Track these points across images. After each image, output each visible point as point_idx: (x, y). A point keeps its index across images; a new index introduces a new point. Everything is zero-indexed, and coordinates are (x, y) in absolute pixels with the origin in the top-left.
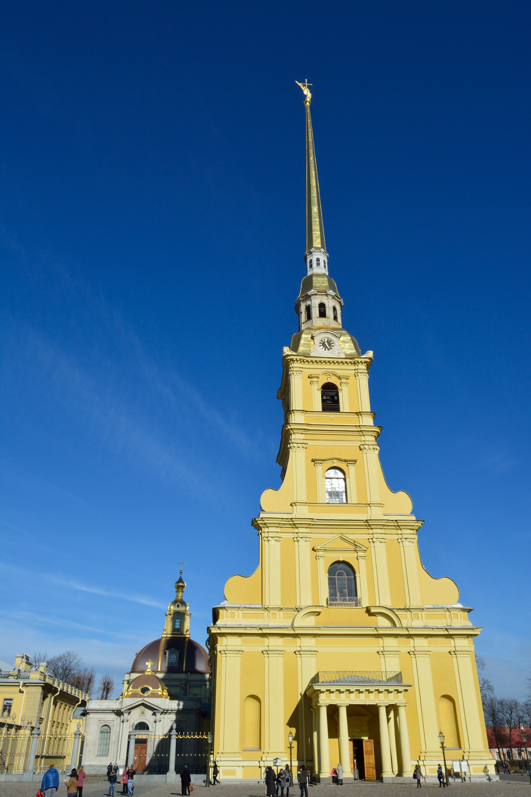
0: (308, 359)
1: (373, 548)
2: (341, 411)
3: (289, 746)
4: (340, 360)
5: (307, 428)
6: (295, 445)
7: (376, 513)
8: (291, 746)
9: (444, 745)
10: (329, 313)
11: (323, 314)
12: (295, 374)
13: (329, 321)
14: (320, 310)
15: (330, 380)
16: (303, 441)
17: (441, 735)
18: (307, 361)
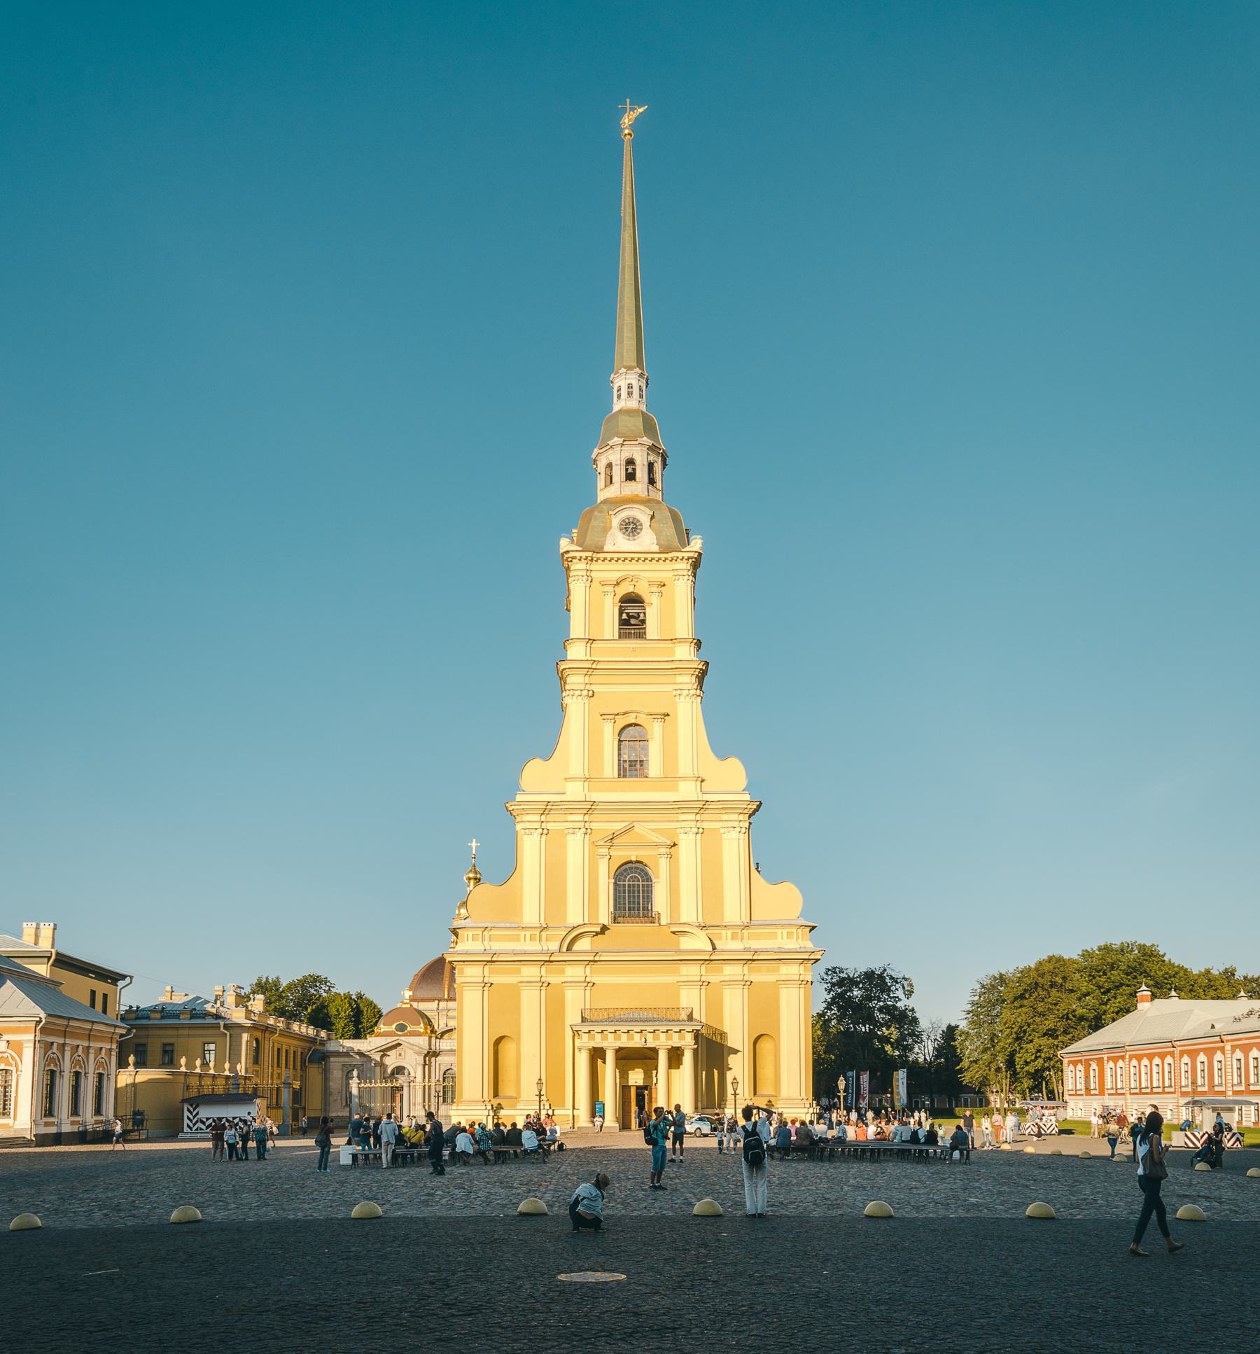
0: (598, 556)
1: (680, 841)
2: (647, 638)
3: (538, 1093)
4: (650, 556)
5: (594, 666)
6: (571, 693)
7: (688, 791)
8: (540, 1094)
9: (737, 1092)
10: (642, 473)
11: (631, 477)
12: (580, 581)
13: (639, 487)
14: (627, 469)
15: (631, 589)
16: (588, 687)
17: (735, 1081)
18: (598, 559)
